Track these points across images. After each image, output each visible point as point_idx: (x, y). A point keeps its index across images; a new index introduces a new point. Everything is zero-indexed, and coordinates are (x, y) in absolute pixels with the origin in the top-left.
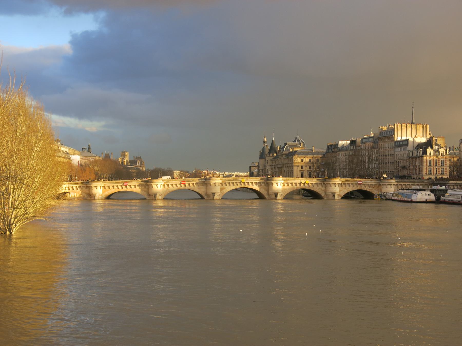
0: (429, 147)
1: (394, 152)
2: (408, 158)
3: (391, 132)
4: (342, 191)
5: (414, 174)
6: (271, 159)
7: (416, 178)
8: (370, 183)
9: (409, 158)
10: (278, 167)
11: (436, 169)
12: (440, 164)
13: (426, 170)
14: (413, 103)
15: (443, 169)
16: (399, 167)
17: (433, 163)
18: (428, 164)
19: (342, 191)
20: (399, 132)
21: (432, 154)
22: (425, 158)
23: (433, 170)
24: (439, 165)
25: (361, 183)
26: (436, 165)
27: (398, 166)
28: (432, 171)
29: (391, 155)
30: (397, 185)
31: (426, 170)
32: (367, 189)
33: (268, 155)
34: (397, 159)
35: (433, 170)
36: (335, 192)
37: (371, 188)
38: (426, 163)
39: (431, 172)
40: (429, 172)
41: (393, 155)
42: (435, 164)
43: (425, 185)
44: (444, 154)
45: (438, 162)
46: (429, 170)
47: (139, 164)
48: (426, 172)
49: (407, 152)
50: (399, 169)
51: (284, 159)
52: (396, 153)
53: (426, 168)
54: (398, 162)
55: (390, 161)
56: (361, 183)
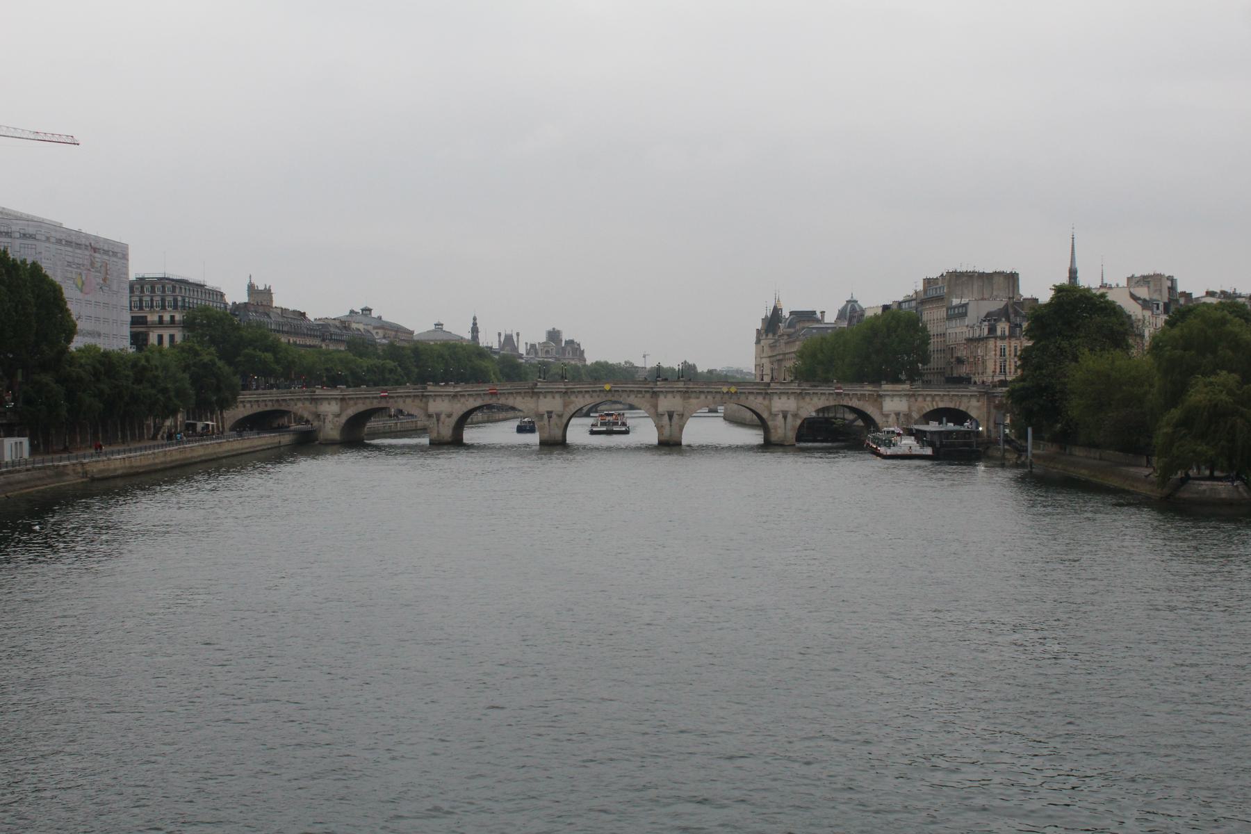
1: (946, 329)
2: (965, 342)
3: (938, 290)
4: (802, 408)
5: (974, 374)
6: (770, 344)
7: (977, 381)
8: (859, 393)
9: (969, 340)
10: (779, 360)
13: (995, 365)
14: (1073, 228)
16: (953, 360)
17: (1010, 351)
18: (998, 353)
19: (802, 408)
21: (1007, 333)
25: (842, 391)
27: (952, 357)
28: (1007, 367)
29: (941, 334)
31: (995, 365)
32: (855, 403)
33: (764, 336)
34: (951, 343)
35: (1010, 365)
36: (787, 409)
37: (861, 403)
38: (995, 351)
39: (1005, 369)
40: (1001, 369)
41: (944, 334)
43: (971, 395)
46: (1001, 366)
47: (569, 353)
48: (995, 369)
49: (965, 329)
50: (952, 363)
51: (786, 343)
52: (949, 331)
53: (993, 361)
54: (952, 348)
55: (936, 347)
56: (842, 391)
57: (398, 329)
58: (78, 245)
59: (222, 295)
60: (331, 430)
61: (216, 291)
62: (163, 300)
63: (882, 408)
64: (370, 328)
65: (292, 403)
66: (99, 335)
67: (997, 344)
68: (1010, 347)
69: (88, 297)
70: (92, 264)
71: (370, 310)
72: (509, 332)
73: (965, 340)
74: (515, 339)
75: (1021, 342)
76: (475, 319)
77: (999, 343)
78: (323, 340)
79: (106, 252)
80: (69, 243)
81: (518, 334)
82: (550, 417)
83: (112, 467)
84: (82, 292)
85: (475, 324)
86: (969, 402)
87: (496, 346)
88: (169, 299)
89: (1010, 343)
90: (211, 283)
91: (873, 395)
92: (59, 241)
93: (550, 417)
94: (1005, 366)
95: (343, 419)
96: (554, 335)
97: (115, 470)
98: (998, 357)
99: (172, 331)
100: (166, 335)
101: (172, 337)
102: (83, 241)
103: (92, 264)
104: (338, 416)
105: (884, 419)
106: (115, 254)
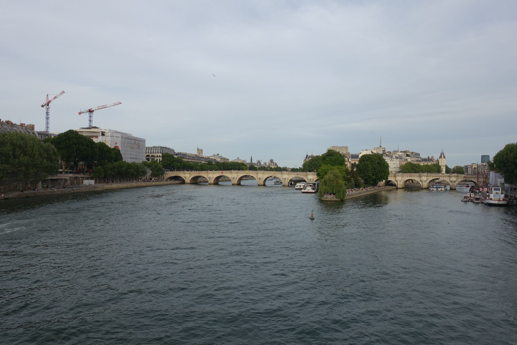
57: (224, 159)
58: (131, 139)
59: (174, 150)
60: (188, 180)
62: (158, 151)
63: (307, 178)
64: (215, 158)
65: (180, 174)
66: (137, 159)
69: (134, 150)
70: (135, 143)
71: (219, 154)
72: (259, 160)
74: (260, 161)
76: (251, 157)
79: (139, 141)
80: (128, 138)
81: (261, 160)
82: (234, 179)
83: (112, 187)
84: (132, 149)
85: (251, 158)
87: (256, 162)
88: (159, 151)
90: (171, 148)
92: (125, 138)
93: (234, 179)
95: (190, 178)
96: (272, 161)
97: (113, 187)
99: (159, 158)
100: (158, 159)
101: (160, 159)
102: (133, 138)
103: (135, 143)
104: (189, 177)
106: (142, 141)
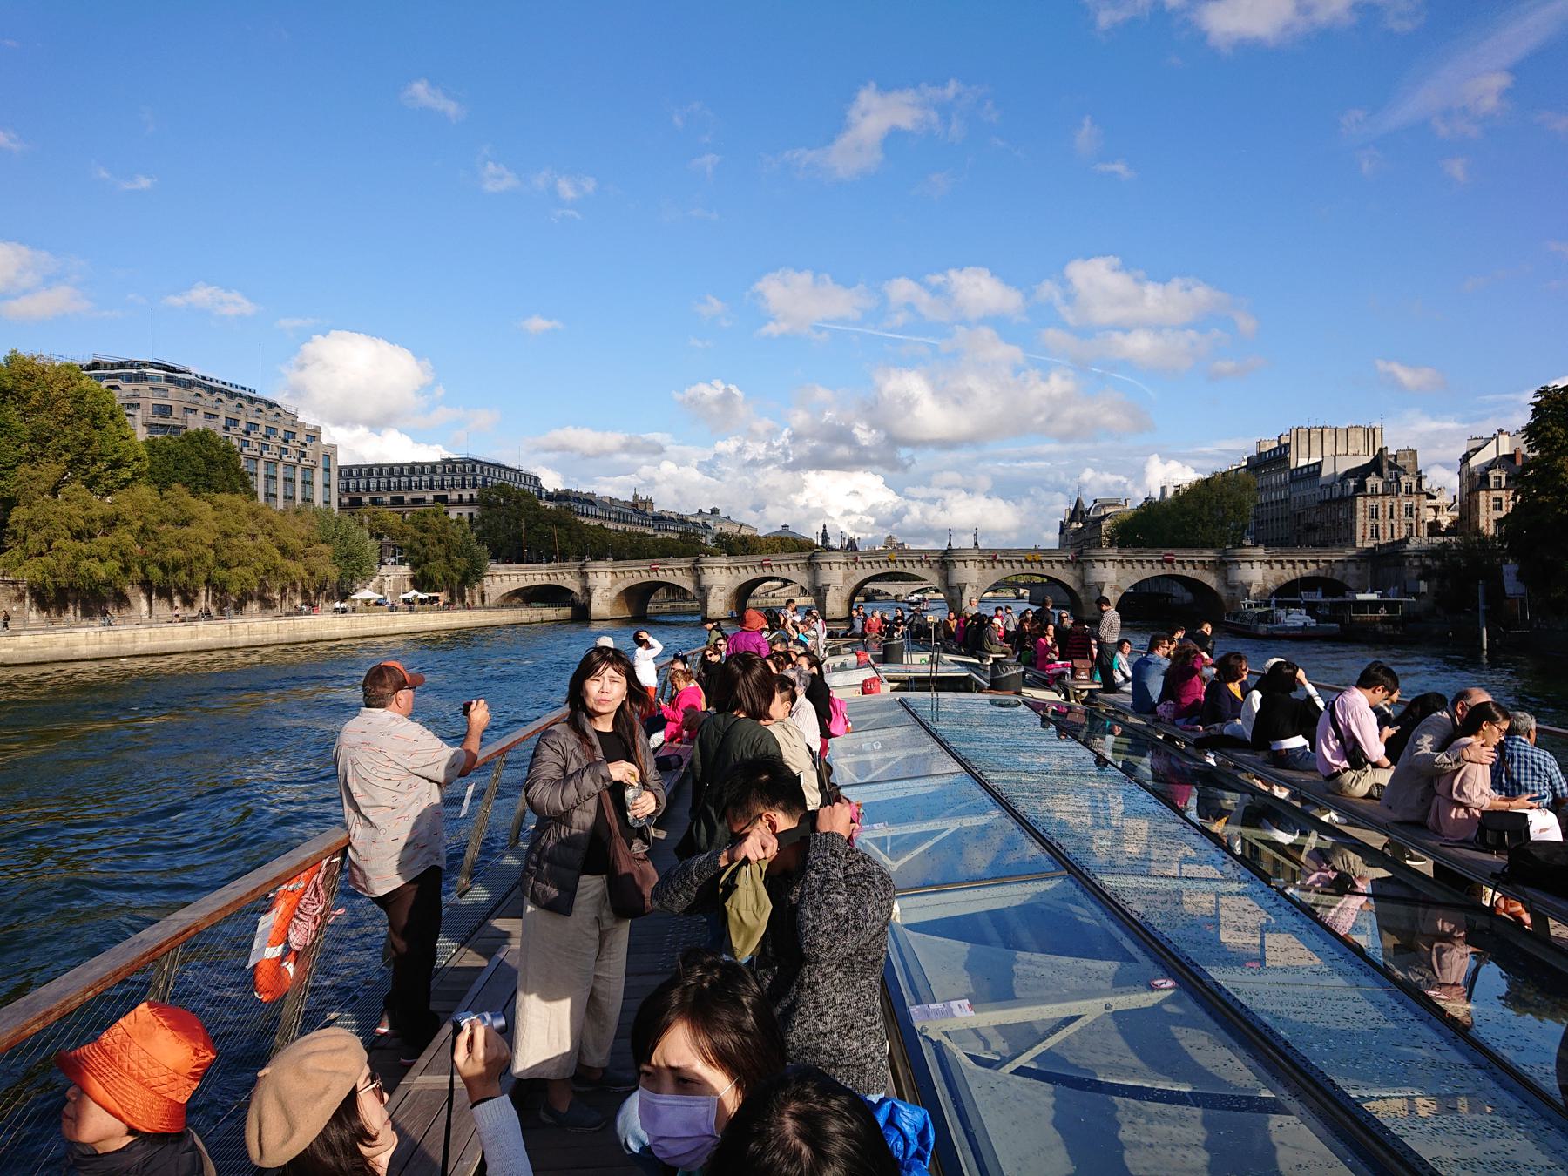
0: (1373, 474)
9: (1322, 502)
11: (1392, 525)
12: (1403, 513)
13: (1365, 529)
15: (1411, 525)
16: (1301, 527)
17: (1384, 511)
18: (1368, 514)
20: (1304, 447)
21: (1380, 491)
22: (1360, 500)
23: (1384, 529)
24: (1399, 515)
26: (1391, 517)
30: (1269, 562)
31: (1365, 529)
32: (1189, 572)
35: (1384, 529)
38: (1365, 511)
42: (1388, 514)
44: (1414, 489)
45: (1395, 508)
48: (1365, 533)
49: (1318, 490)
59: (537, 479)
61: (531, 476)
67: (1368, 504)
68: (1384, 506)
73: (1319, 502)
75: (1399, 501)
76: (824, 526)
77: (1370, 502)
78: (659, 530)
86: (1345, 569)
89: (1384, 502)
91: (1214, 562)
94: (1377, 530)
98: (1368, 519)
105: (1229, 592)
